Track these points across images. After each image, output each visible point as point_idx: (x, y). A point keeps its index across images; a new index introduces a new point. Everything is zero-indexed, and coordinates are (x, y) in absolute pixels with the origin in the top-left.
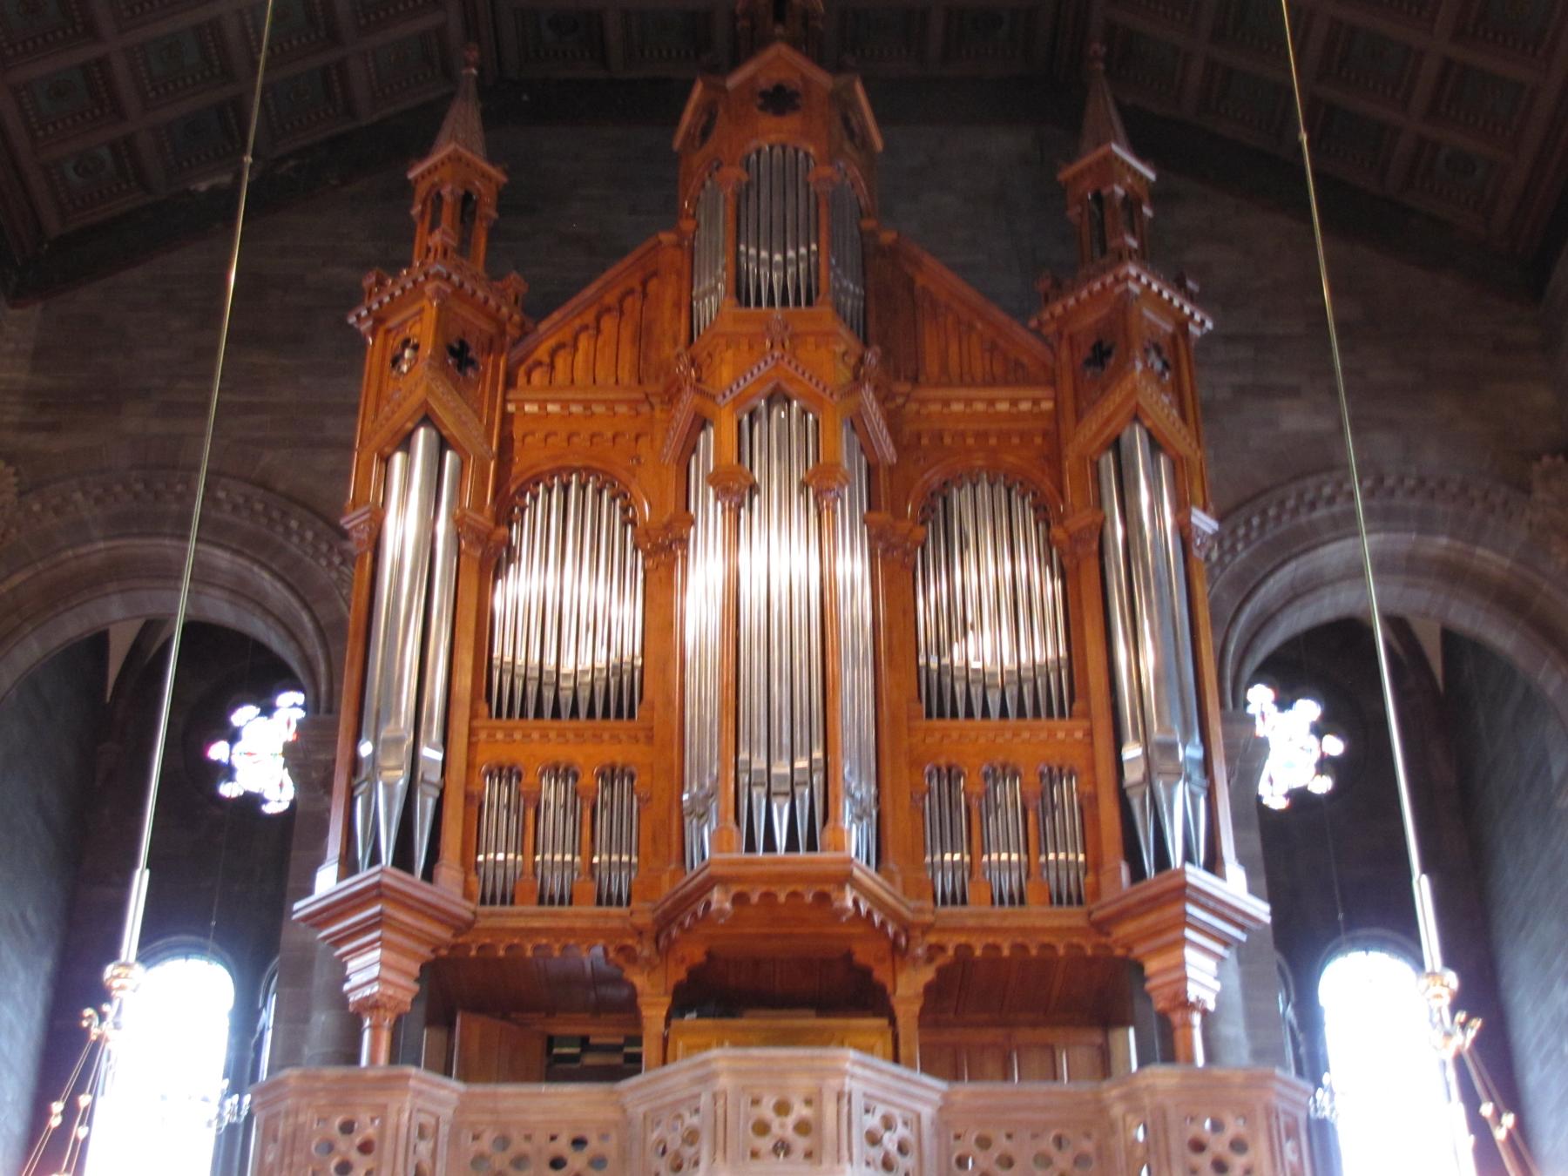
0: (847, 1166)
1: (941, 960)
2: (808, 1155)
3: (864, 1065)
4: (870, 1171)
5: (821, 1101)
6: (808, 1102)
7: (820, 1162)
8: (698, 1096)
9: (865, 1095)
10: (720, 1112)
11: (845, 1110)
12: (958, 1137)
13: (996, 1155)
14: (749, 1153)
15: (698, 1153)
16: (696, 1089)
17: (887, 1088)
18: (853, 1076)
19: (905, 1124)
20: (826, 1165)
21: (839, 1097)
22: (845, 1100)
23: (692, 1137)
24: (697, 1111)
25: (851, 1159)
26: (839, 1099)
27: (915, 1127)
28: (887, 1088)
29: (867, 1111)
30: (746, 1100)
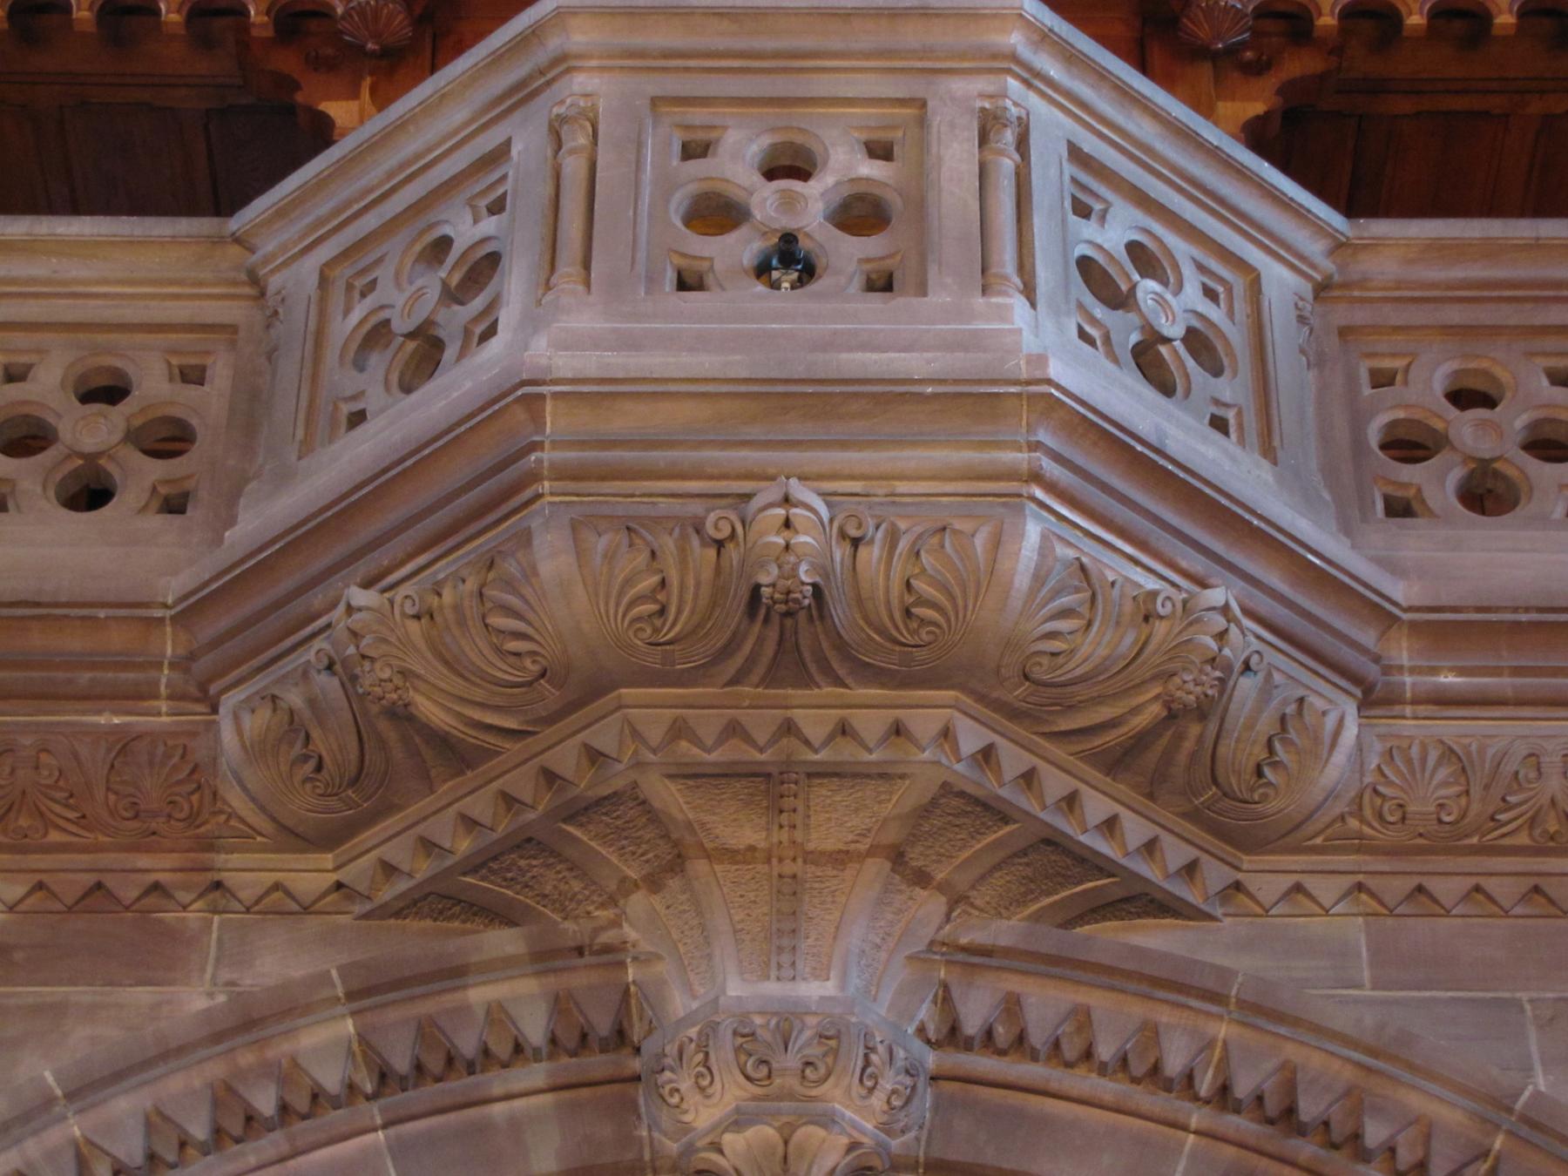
0: (1019, 303)
1: (1298, 65)
2: (882, 283)
3: (1071, 58)
4: (1098, 356)
5: (923, 146)
6: (880, 151)
7: (922, 290)
8: (501, 153)
9: (1076, 154)
10: (573, 168)
11: (1007, 164)
12: (1382, 379)
13: (1521, 422)
14: (670, 277)
15: (492, 306)
16: (487, 142)
17: (1143, 155)
18: (1033, 78)
19: (1210, 294)
20: (939, 297)
21: (988, 126)
22: (1009, 136)
23: (485, 266)
24: (497, 208)
25: (1029, 292)
26: (983, 139)
27: (1241, 307)
28: (1143, 155)
29: (1083, 211)
30: (661, 144)
